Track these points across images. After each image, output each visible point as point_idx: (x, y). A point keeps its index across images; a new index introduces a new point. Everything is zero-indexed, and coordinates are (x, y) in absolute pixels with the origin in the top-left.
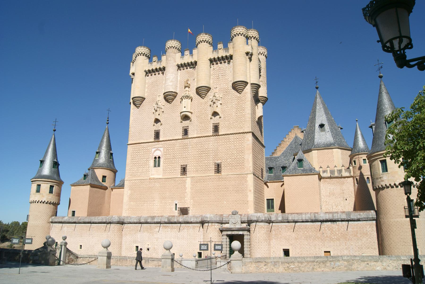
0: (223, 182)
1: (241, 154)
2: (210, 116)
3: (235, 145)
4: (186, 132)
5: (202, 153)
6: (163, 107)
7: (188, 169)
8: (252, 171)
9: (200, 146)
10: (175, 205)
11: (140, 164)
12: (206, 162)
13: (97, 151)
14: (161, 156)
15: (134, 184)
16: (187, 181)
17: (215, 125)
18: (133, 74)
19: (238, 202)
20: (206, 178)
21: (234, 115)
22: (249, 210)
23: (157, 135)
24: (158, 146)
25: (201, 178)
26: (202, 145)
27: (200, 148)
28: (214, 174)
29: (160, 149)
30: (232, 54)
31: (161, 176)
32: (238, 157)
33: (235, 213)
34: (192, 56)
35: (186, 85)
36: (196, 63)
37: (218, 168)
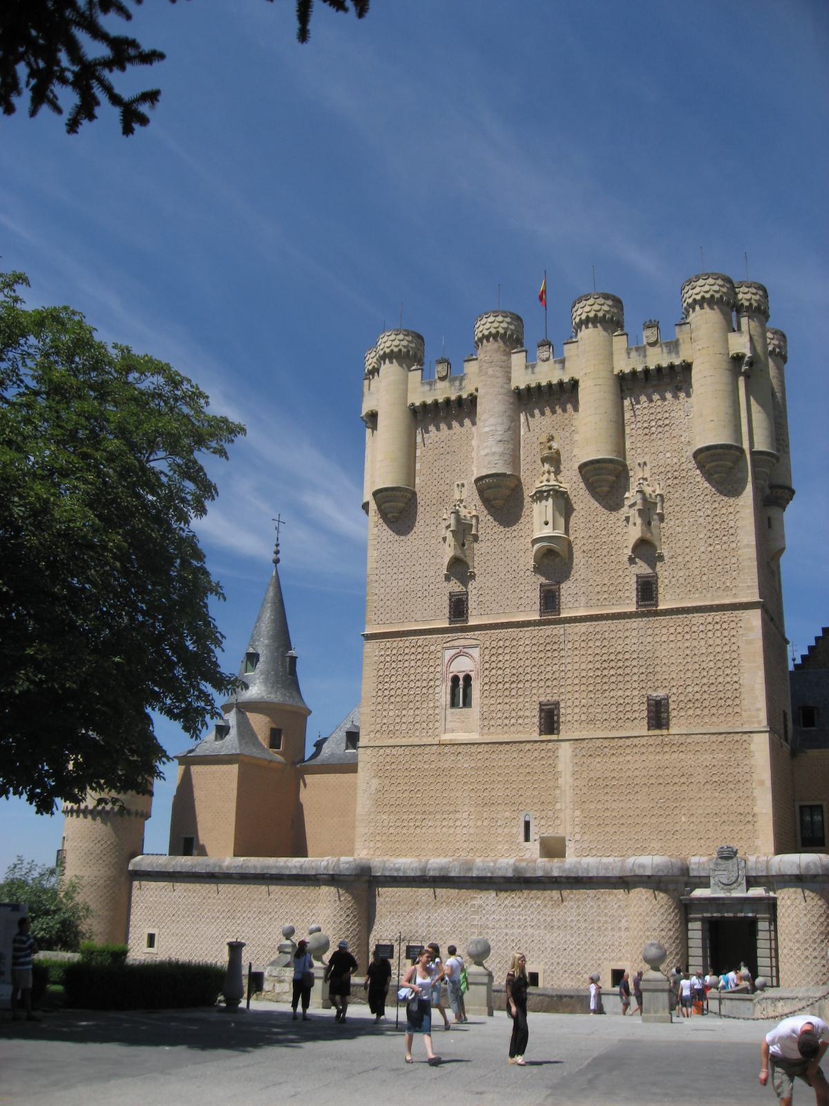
0: (675, 755)
1: (728, 671)
2: (629, 552)
3: (711, 642)
4: (550, 600)
5: (605, 665)
7: (567, 713)
8: (765, 722)
9: (598, 643)
10: (523, 825)
11: (405, 698)
12: (620, 693)
13: (251, 650)
14: (472, 674)
15: (388, 759)
16: (561, 752)
18: (373, 417)
19: (725, 818)
20: (621, 742)
21: (703, 549)
22: (758, 842)
23: (458, 608)
24: (462, 642)
25: (606, 743)
26: (605, 643)
27: (598, 651)
28: (645, 732)
29: (470, 651)
30: (689, 361)
31: (475, 737)
32: (720, 679)
33: (728, 855)
34: (562, 362)
35: (546, 452)
36: (575, 384)
37: (658, 715)
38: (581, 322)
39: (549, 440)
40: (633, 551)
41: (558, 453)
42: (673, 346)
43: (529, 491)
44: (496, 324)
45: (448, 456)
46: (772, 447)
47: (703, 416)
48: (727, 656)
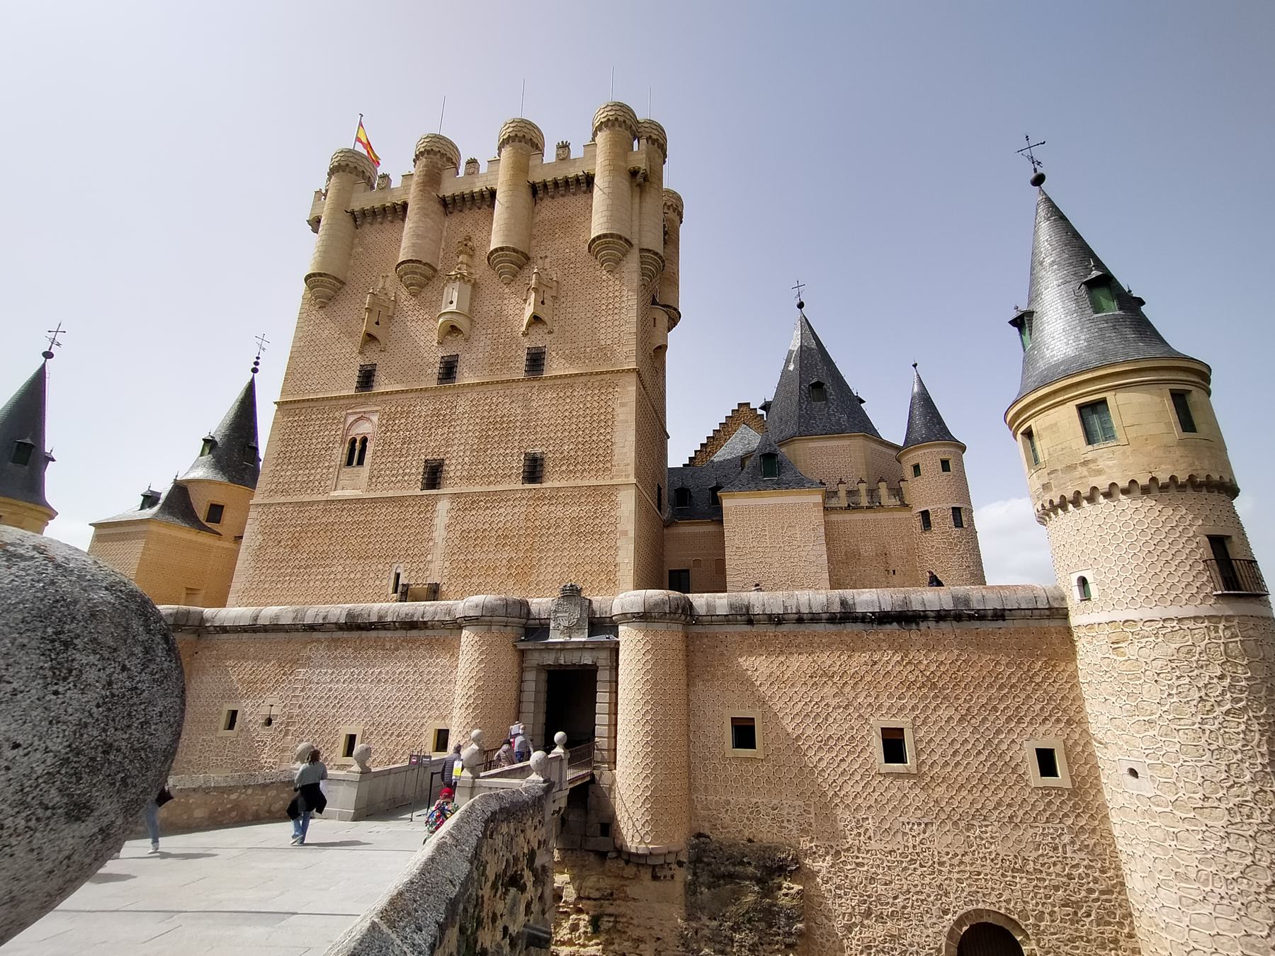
10: (393, 576)
27: (486, 414)
28: (520, 486)
32: (594, 438)
37: (534, 470)
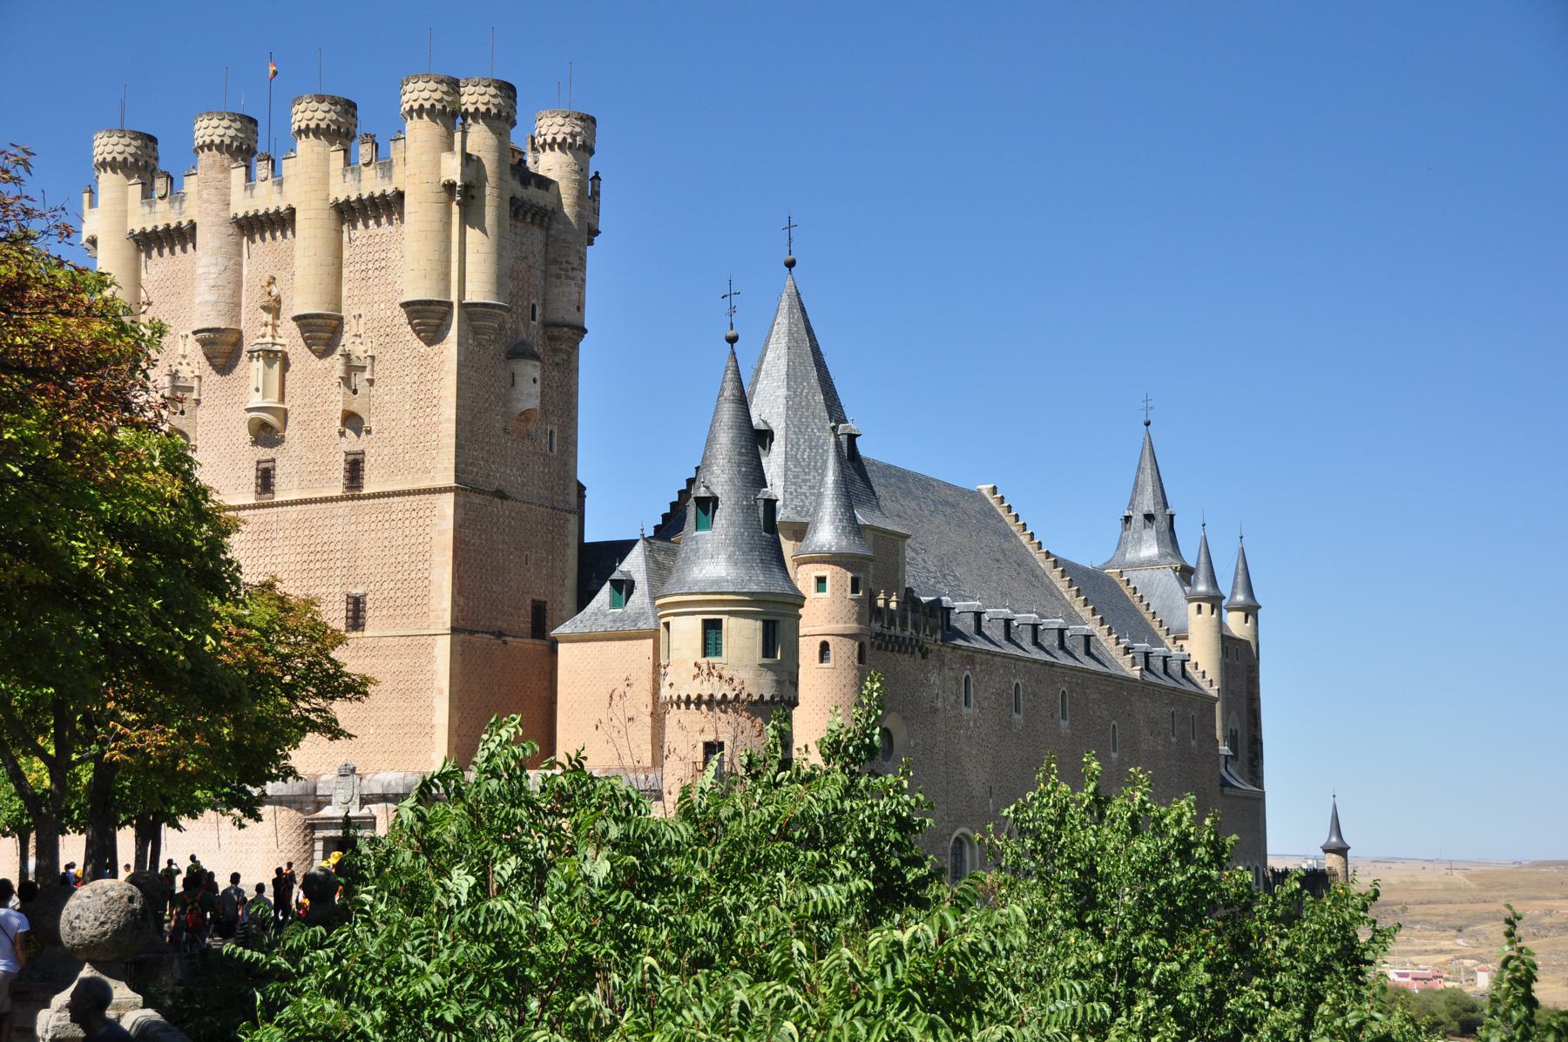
6: (195, 384)
17: (351, 458)
18: (93, 242)
34: (280, 184)
38: (300, 131)
39: (269, 284)
40: (344, 423)
41: (278, 301)
42: (386, 167)
43: (246, 347)
44: (210, 131)
45: (173, 299)
46: (498, 294)
47: (409, 258)
48: (421, 548)
